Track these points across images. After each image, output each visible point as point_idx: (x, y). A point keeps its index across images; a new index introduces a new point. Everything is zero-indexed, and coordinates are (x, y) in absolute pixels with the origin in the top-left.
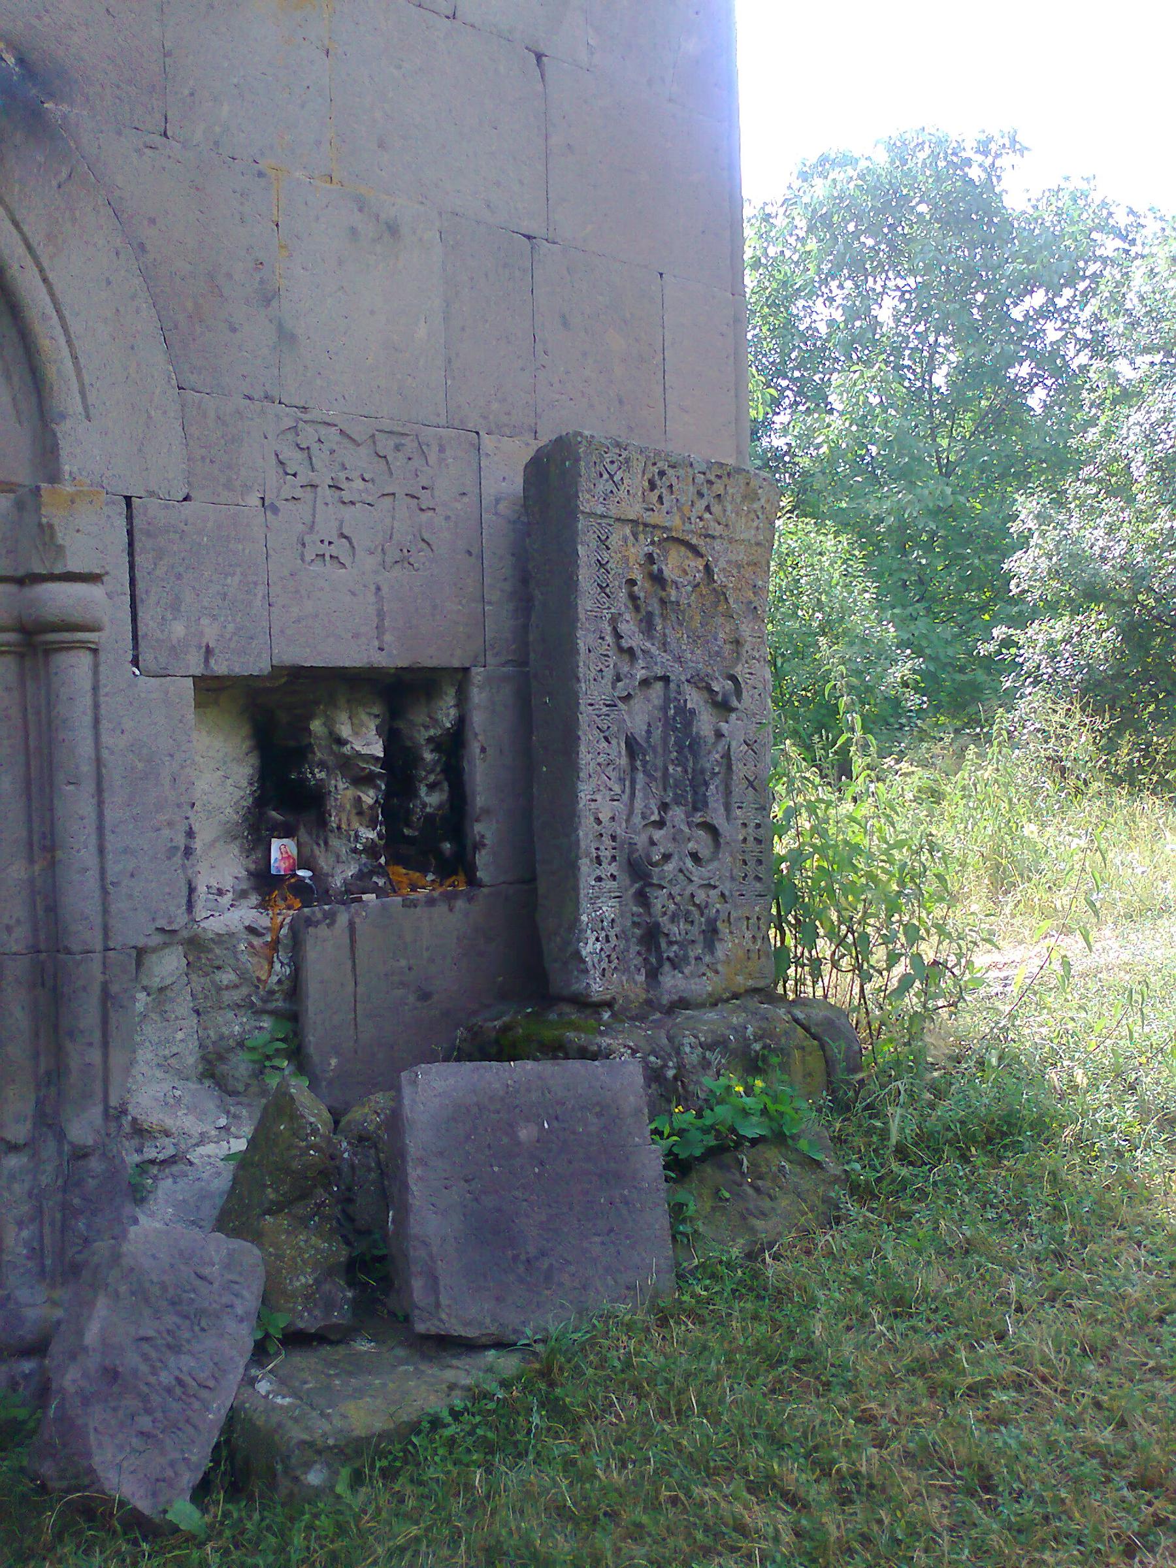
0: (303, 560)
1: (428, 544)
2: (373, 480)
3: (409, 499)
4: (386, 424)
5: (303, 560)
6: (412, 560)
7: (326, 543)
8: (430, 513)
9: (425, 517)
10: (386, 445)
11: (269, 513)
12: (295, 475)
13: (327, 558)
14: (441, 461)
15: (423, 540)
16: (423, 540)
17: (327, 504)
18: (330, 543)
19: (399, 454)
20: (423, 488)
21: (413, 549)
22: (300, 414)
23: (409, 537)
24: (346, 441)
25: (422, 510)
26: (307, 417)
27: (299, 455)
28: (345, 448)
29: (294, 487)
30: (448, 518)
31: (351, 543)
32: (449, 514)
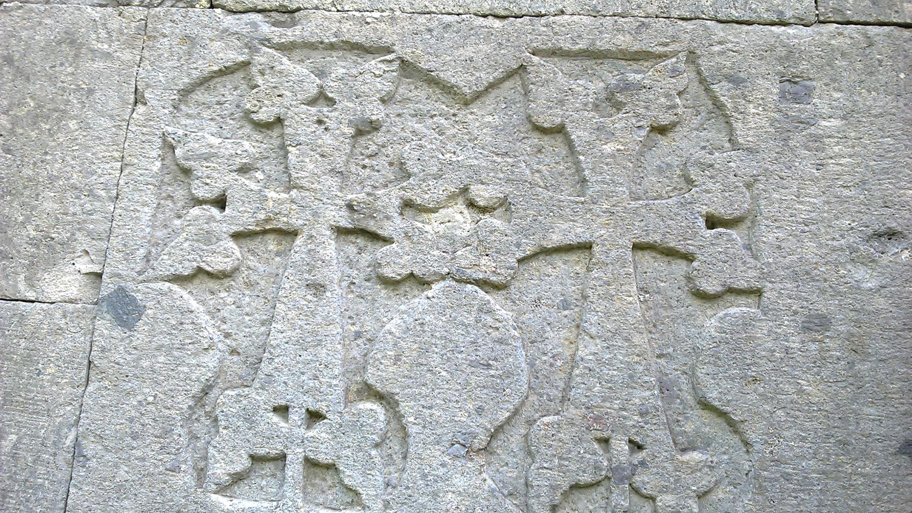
0: (201, 474)
1: (732, 425)
2: (504, 204)
3: (650, 263)
4: (576, 30)
5: (201, 474)
6: (645, 480)
7: (297, 416)
8: (738, 309)
9: (710, 322)
10: (566, 93)
11: (104, 325)
12: (221, 203)
13: (294, 469)
14: (787, 129)
15: (705, 405)
16: (705, 405)
17: (318, 288)
18: (314, 416)
19: (618, 122)
20: (712, 222)
21: (657, 436)
22: (266, 29)
23: (639, 396)
24: (421, 94)
25: (702, 296)
26: (291, 34)
27: (250, 146)
28: (418, 115)
29: (208, 238)
30: (817, 324)
31: (395, 415)
32: (822, 306)
